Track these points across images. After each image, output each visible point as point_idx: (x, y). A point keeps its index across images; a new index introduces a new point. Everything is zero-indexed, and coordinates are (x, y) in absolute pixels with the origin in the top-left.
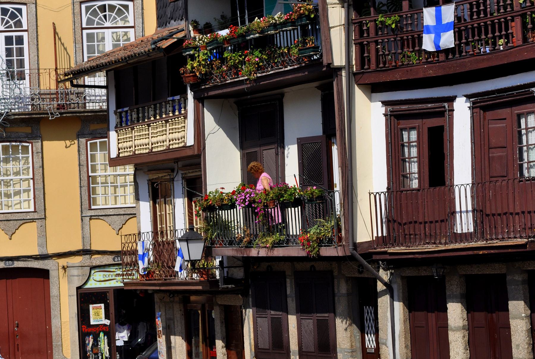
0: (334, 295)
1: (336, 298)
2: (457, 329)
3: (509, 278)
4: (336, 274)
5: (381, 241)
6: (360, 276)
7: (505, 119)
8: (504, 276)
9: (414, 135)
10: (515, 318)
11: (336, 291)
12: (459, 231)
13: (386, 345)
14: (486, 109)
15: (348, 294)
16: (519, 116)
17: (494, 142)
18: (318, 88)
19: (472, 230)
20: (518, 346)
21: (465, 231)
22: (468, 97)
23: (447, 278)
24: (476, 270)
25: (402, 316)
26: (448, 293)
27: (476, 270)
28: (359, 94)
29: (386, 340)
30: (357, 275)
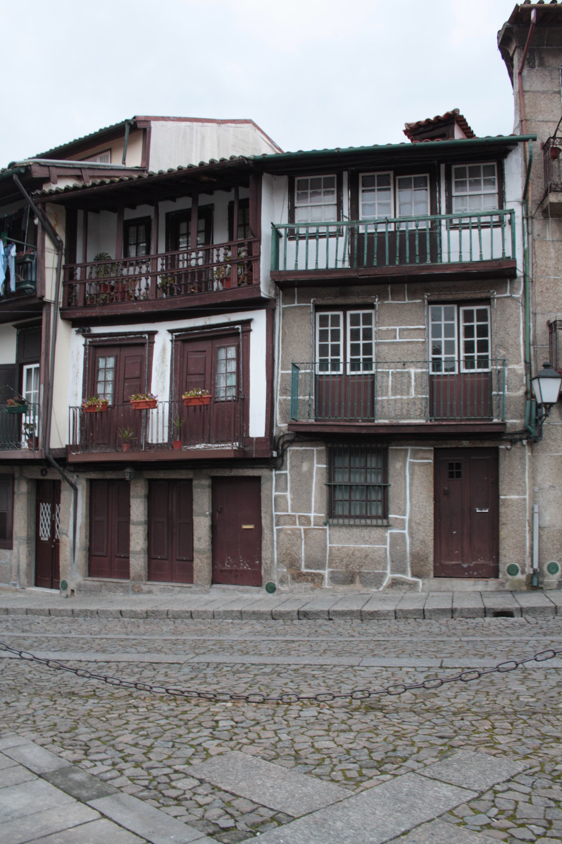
0: (13, 493)
1: (15, 496)
2: (138, 524)
3: (195, 482)
4: (17, 476)
5: (69, 449)
6: (42, 478)
7: (205, 351)
8: (191, 480)
9: (111, 362)
10: (199, 515)
11: (16, 490)
12: (155, 442)
13: (67, 535)
14: (184, 341)
15: (28, 493)
16: (220, 348)
17: (192, 369)
18: (15, 326)
19: (166, 441)
20: (199, 539)
21: (160, 441)
22: (171, 332)
23: (132, 482)
24: (161, 475)
25: (84, 512)
26: (132, 494)
27: (161, 475)
28: (62, 326)
29: (67, 531)
30: (40, 477)
